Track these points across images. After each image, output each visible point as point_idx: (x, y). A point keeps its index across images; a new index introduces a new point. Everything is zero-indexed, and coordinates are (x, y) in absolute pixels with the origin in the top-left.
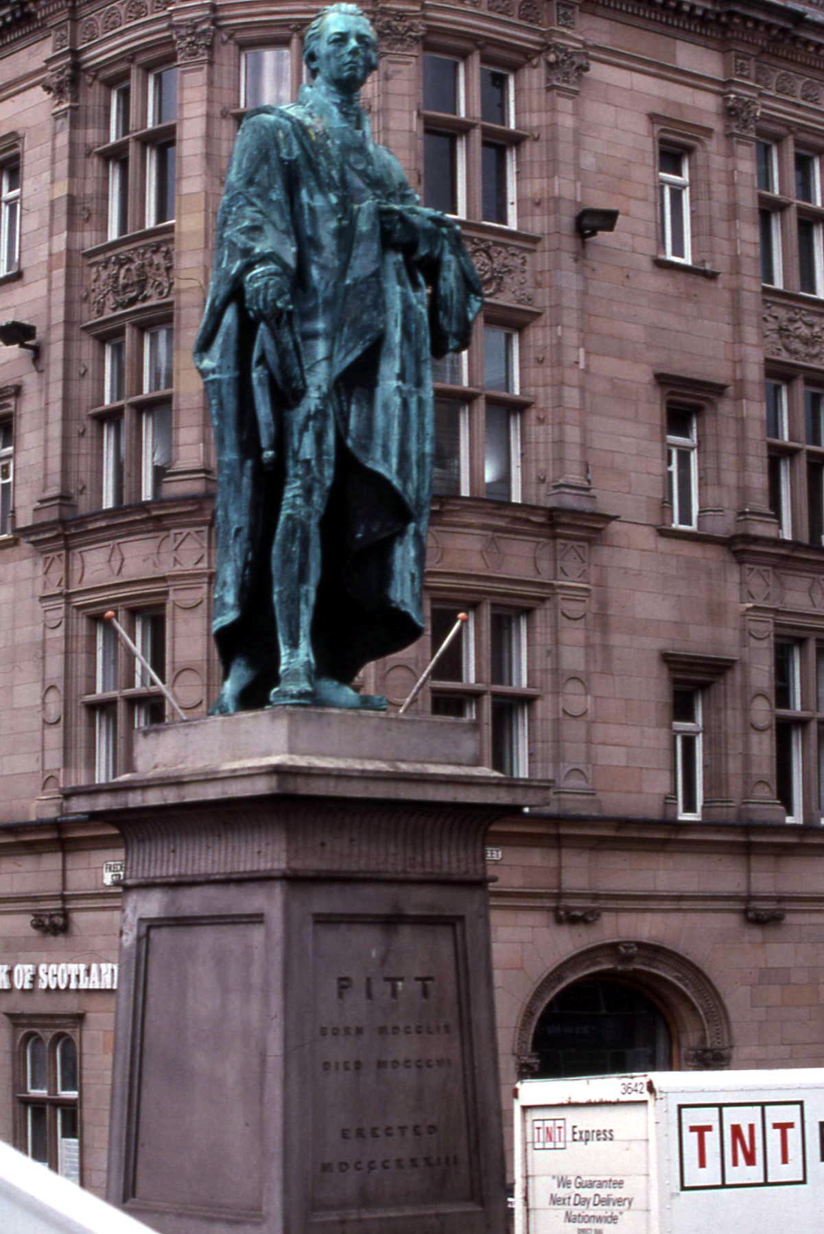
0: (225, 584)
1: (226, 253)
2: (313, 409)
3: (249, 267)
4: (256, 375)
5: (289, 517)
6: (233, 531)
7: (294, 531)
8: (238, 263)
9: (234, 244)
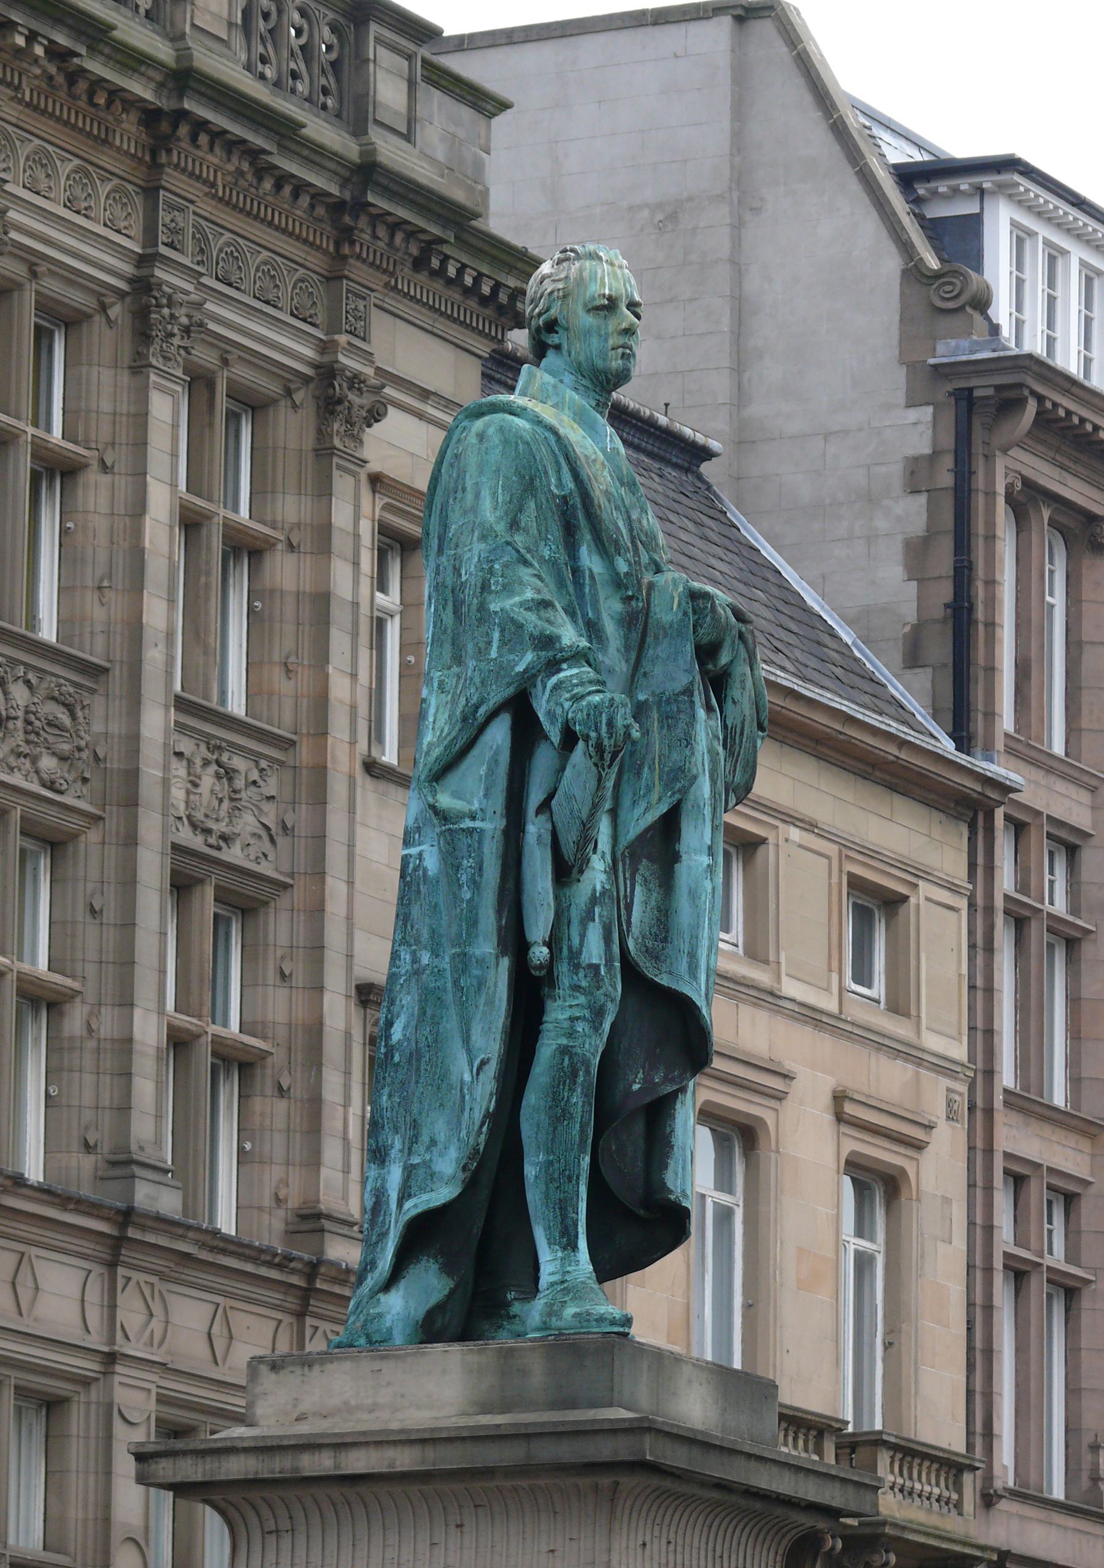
0: (433, 1142)
1: (496, 635)
2: (599, 888)
3: (553, 666)
4: (535, 829)
5: (564, 1051)
6: (476, 1064)
7: (574, 1074)
8: (529, 657)
9: (520, 626)
